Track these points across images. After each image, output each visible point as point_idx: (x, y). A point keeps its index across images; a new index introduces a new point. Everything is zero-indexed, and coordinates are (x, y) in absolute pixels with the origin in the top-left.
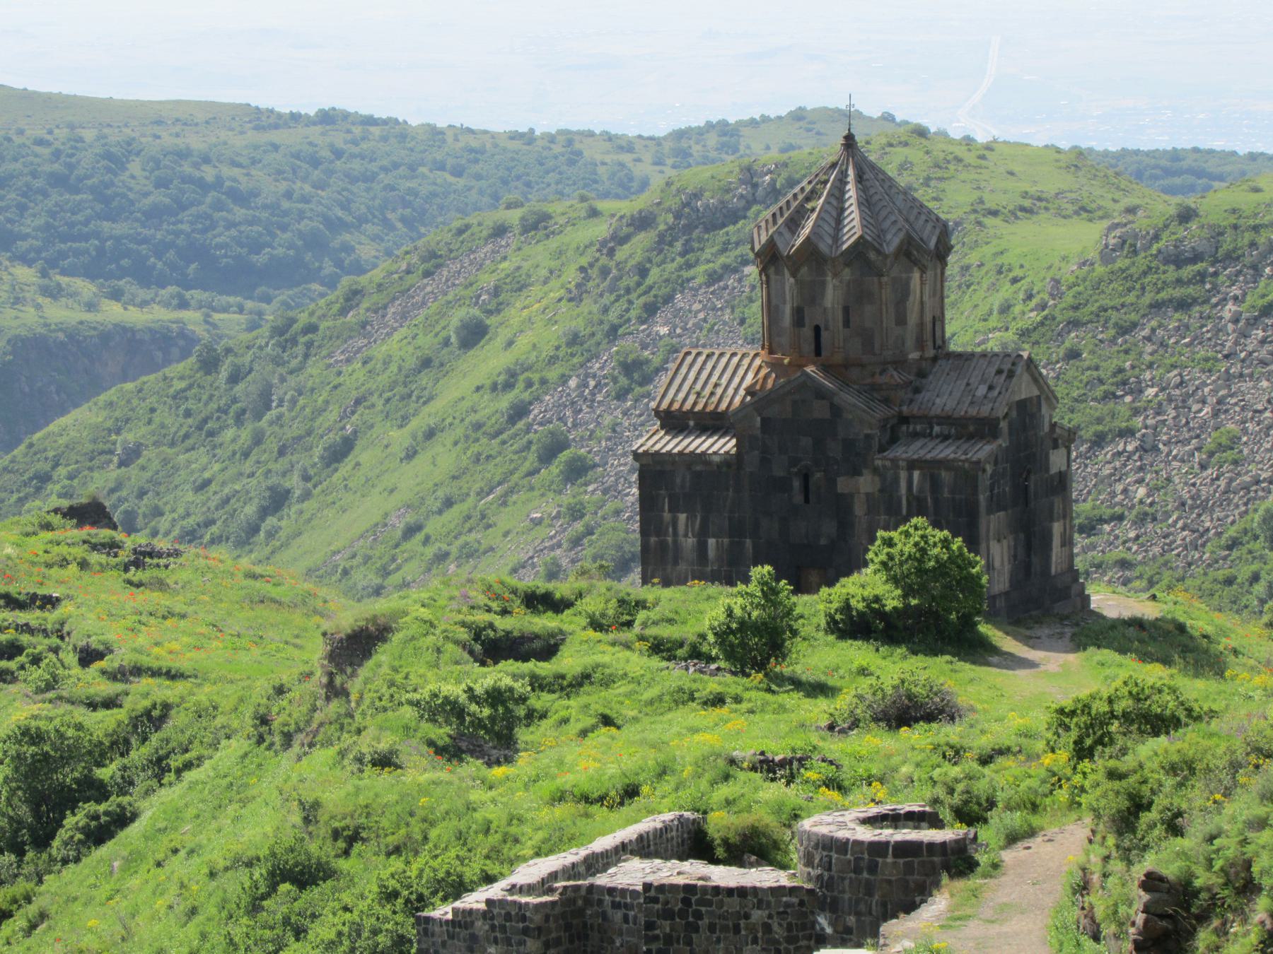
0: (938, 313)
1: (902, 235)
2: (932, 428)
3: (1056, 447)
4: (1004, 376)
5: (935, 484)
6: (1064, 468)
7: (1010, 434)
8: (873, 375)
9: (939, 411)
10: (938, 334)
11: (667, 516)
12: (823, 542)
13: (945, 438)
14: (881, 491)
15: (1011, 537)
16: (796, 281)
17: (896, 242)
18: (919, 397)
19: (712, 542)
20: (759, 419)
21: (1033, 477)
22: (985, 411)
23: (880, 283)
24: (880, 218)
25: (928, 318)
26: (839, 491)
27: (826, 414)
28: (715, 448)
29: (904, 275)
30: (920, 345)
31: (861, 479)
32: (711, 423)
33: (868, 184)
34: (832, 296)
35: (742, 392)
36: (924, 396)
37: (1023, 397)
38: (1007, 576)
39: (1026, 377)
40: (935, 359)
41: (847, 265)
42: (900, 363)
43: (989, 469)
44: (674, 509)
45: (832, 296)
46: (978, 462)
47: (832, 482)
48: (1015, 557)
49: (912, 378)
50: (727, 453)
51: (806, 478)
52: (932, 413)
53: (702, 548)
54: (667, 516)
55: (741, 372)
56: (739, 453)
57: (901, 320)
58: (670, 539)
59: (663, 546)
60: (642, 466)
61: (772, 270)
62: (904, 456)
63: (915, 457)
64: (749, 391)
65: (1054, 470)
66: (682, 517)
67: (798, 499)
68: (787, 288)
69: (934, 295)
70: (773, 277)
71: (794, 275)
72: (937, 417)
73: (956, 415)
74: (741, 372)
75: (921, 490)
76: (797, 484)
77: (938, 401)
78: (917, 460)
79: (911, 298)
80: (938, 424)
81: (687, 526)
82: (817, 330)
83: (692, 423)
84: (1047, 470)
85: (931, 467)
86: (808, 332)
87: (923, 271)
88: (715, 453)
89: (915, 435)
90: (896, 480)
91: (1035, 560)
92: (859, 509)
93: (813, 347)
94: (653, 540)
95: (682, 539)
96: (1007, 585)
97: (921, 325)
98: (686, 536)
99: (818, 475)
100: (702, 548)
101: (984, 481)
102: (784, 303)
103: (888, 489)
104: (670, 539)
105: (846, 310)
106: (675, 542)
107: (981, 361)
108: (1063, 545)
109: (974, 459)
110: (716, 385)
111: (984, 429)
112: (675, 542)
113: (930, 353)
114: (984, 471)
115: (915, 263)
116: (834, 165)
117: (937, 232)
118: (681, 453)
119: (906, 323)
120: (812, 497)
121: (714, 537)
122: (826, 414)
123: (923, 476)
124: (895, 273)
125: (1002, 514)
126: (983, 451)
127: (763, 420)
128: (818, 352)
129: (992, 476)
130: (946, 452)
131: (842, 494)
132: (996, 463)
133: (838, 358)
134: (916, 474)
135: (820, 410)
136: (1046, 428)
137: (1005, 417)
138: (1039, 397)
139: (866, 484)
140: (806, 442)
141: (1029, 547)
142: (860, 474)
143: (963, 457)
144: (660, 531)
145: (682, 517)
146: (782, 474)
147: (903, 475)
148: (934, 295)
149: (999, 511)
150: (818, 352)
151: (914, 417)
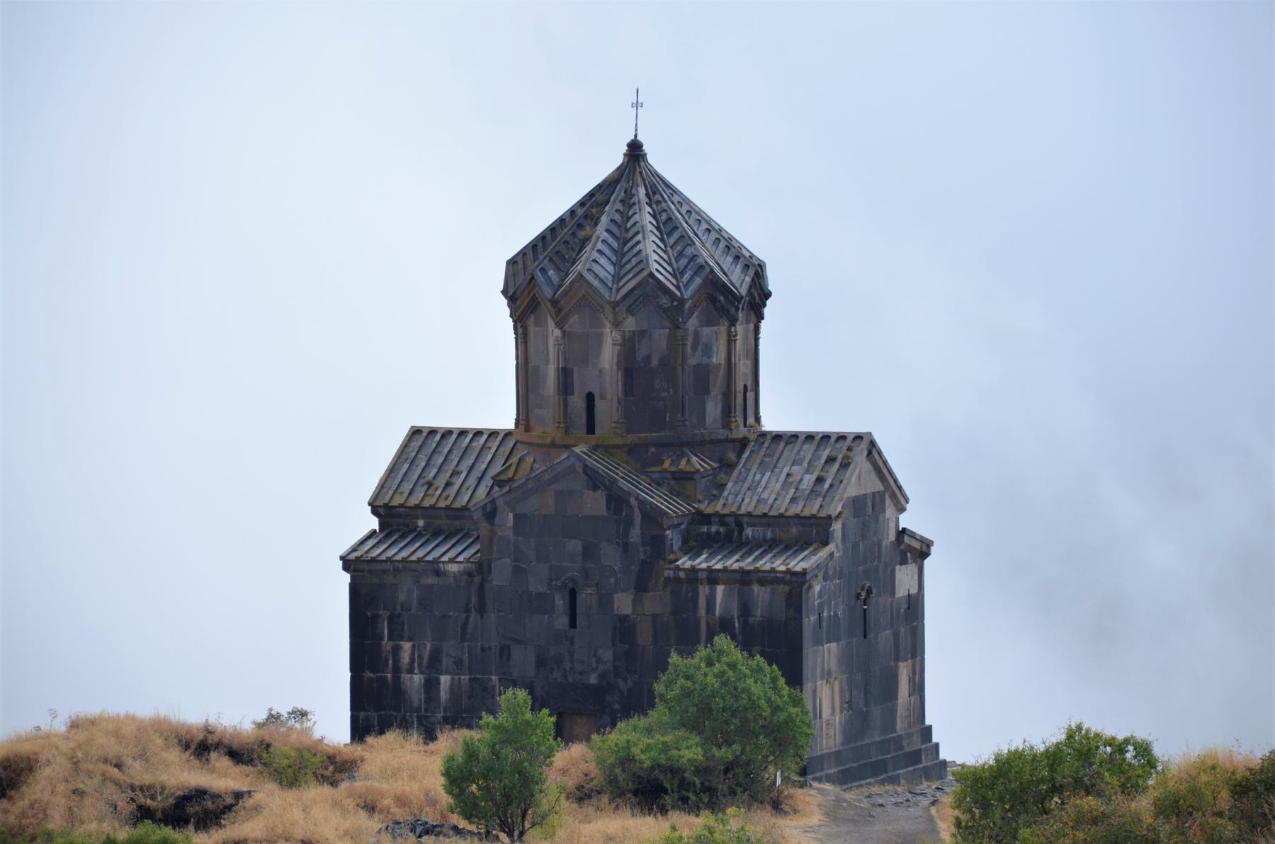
3: (904, 562)
4: (836, 466)
6: (914, 591)
16: (564, 333)
17: (698, 281)
19: (445, 680)
20: (511, 515)
22: (813, 508)
35: (488, 482)
39: (867, 466)
41: (630, 311)
46: (804, 573)
48: (850, 703)
53: (431, 686)
54: (387, 645)
64: (498, 482)
65: (901, 592)
66: (407, 646)
67: (562, 622)
68: (551, 343)
70: (532, 329)
71: (559, 325)
72: (749, 514)
76: (560, 602)
80: (750, 525)
81: (413, 654)
82: (590, 398)
83: (421, 523)
86: (578, 402)
91: (876, 711)
93: (583, 421)
95: (405, 677)
96: (839, 739)
98: (411, 671)
100: (431, 686)
102: (547, 363)
106: (397, 679)
111: (813, 531)
113: (741, 432)
117: (751, 272)
120: (580, 620)
121: (447, 673)
123: (727, 595)
125: (833, 645)
127: (515, 516)
128: (591, 429)
129: (820, 592)
134: (720, 589)
136: (892, 537)
137: (838, 517)
138: (881, 495)
140: (575, 545)
145: (407, 646)
146: (541, 589)
151: (716, 514)
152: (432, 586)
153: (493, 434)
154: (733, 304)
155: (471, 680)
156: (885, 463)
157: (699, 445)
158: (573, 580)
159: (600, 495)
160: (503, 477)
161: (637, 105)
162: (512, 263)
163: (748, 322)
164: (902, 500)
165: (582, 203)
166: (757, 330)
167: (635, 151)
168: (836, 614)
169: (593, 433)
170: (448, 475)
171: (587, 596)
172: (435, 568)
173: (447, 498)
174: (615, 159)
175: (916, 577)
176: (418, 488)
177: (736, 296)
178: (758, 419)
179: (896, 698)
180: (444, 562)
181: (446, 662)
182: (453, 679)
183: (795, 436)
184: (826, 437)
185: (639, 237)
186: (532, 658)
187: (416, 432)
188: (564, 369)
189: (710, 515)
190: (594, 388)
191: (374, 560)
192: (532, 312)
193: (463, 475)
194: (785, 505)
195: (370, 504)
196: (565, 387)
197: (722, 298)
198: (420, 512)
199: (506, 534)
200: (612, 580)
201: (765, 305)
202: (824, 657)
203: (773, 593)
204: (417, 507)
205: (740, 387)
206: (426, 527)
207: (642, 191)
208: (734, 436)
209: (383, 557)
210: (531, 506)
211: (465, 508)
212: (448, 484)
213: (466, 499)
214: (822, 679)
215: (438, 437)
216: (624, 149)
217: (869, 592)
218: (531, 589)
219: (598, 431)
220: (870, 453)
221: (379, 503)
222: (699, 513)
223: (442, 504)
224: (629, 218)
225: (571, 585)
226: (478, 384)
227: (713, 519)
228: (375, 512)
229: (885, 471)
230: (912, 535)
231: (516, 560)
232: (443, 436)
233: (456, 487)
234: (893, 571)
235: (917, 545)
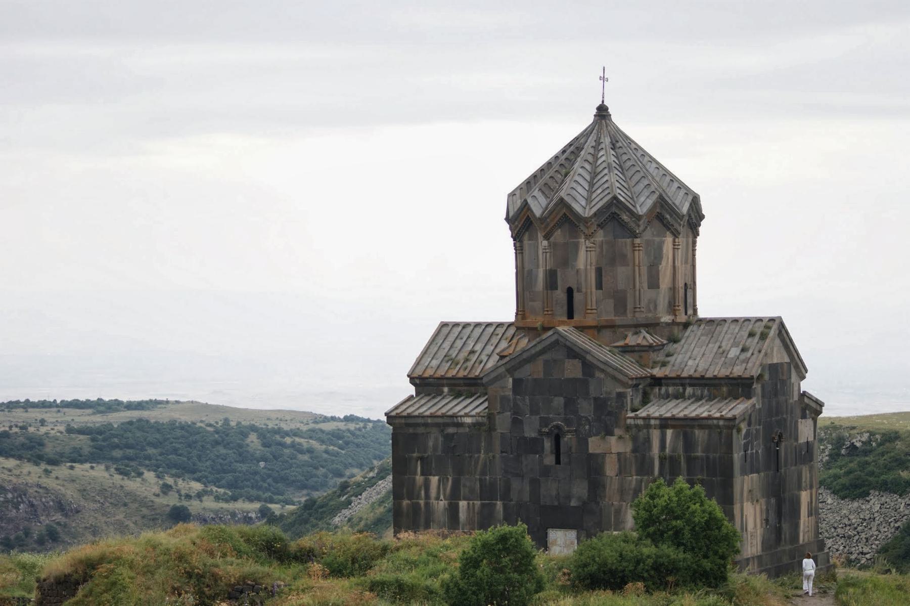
0: (689, 283)
1: (655, 197)
2: (685, 390)
3: (804, 417)
5: (689, 445)
6: (811, 439)
7: (763, 397)
8: (625, 337)
9: (691, 372)
10: (690, 300)
12: (573, 503)
13: (699, 399)
14: (634, 450)
15: (763, 501)
17: (649, 203)
18: (671, 359)
19: (463, 504)
20: (511, 380)
21: (783, 444)
23: (633, 245)
24: (633, 183)
25: (680, 284)
26: (590, 451)
27: (579, 375)
28: (467, 410)
29: (657, 239)
30: (672, 308)
31: (613, 440)
32: (466, 386)
33: (620, 151)
34: (585, 258)
36: (677, 359)
37: (775, 361)
38: (759, 540)
39: (778, 342)
40: (686, 325)
41: (601, 226)
42: (652, 326)
43: (744, 427)
44: (426, 473)
45: (585, 258)
46: (734, 419)
47: (583, 442)
48: (767, 520)
49: (665, 342)
50: (478, 414)
51: (557, 440)
52: (685, 375)
53: (453, 510)
54: (419, 479)
55: (495, 340)
56: (490, 417)
57: (654, 284)
58: (422, 502)
59: (415, 508)
60: (394, 429)
61: (526, 237)
62: (657, 414)
63: (669, 415)
65: (802, 440)
66: (434, 480)
67: (550, 460)
68: (540, 252)
69: (686, 262)
70: (526, 242)
71: (547, 237)
72: (690, 377)
73: (709, 375)
74: (495, 340)
75: (674, 450)
76: (548, 444)
77: (690, 363)
78: (673, 418)
79: (664, 263)
80: (691, 385)
82: (570, 291)
83: (446, 389)
84: (797, 439)
85: (685, 426)
86: (560, 295)
87: (676, 234)
88: (467, 415)
89: (667, 397)
90: (648, 440)
91: (785, 526)
92: (611, 469)
93: (565, 308)
94: (405, 502)
95: (433, 501)
96: (759, 548)
97: (673, 289)
98: (438, 498)
100: (453, 510)
101: (739, 441)
102: (538, 267)
103: (641, 448)
104: (422, 502)
105: (599, 271)
106: (427, 504)
107: (733, 326)
108: (810, 514)
109: (729, 415)
110: (472, 352)
111: (739, 387)
112: (427, 504)
113: (682, 318)
114: (739, 430)
115: (667, 227)
116: (586, 134)
117: (690, 198)
118: (432, 416)
119: (658, 287)
121: (465, 499)
122: (579, 375)
123: (676, 437)
124: (648, 235)
126: (738, 408)
127: (514, 381)
128: (570, 315)
130: (701, 410)
131: (591, 454)
132: (749, 424)
133: (590, 321)
134: (669, 433)
135: (573, 370)
136: (796, 398)
138: (789, 364)
139: (615, 446)
140: (559, 401)
141: (779, 514)
142: (612, 434)
143: (718, 415)
144: (412, 494)
145: (434, 480)
146: (533, 435)
147: (655, 435)
148: (686, 262)
149: (752, 473)
150: (570, 315)
151: (666, 378)
152: (453, 434)
153: (500, 325)
154: (676, 221)
155: (483, 505)
156: (791, 340)
157: (652, 326)
158: (558, 427)
159: (577, 363)
160: (505, 353)
161: (603, 79)
162: (512, 195)
163: (687, 236)
164: (803, 370)
165: (564, 151)
166: (694, 243)
167: (602, 112)
168: (757, 452)
169: (572, 318)
170: (466, 354)
171: (568, 439)
172: (453, 421)
173: (466, 369)
174: (587, 119)
175: (812, 429)
176: (444, 364)
177: (679, 217)
178: (695, 311)
179: (799, 518)
180: (461, 416)
181: (463, 491)
183: (724, 320)
184: (748, 320)
185: (606, 171)
186: (527, 488)
187: (444, 325)
188: (551, 270)
189: (660, 379)
190: (573, 284)
191: (409, 416)
192: (527, 230)
193: (477, 354)
194: (718, 369)
195: (408, 376)
197: (668, 216)
198: (445, 382)
199: (507, 393)
200: (587, 427)
201: (700, 225)
202: (746, 483)
203: (710, 435)
204: (442, 378)
206: (450, 391)
207: (607, 141)
208: (678, 320)
209: (416, 413)
210: (526, 372)
211: (476, 378)
212: (467, 360)
213: (479, 371)
214: (748, 500)
215: (460, 328)
216: (595, 111)
217: (780, 437)
218: (527, 435)
219: (577, 317)
220: (780, 332)
221: (415, 375)
222: (653, 377)
223: (461, 375)
224: (597, 159)
225: (556, 431)
226: (486, 286)
227: (663, 381)
229: (791, 347)
230: (810, 398)
231: (515, 413)
232: (464, 327)
233: (472, 362)
234: (796, 422)
235: (813, 405)
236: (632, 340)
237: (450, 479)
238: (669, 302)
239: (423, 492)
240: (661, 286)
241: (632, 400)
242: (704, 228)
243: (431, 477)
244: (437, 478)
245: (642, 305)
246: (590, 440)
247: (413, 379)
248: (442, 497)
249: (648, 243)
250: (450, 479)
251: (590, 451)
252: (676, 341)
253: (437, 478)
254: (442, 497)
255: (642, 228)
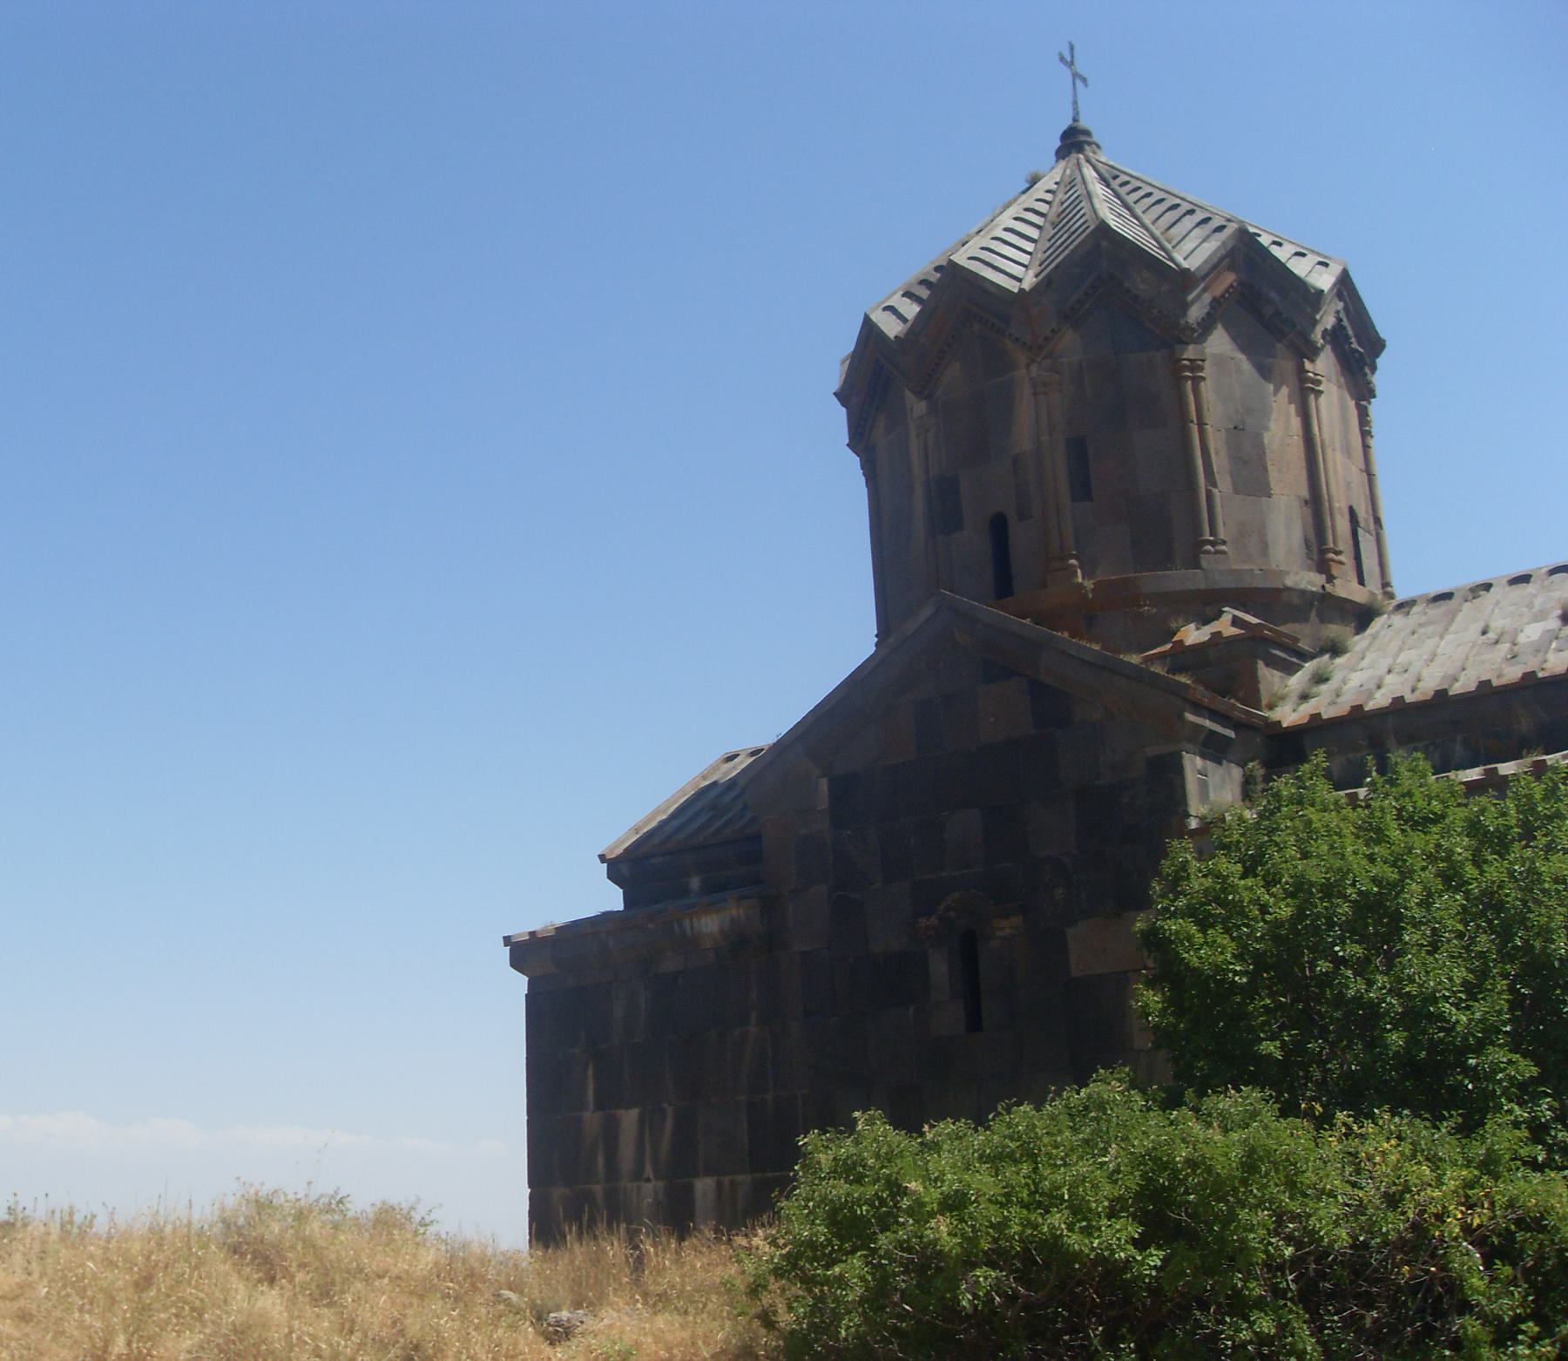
11: (591, 1119)
20: (824, 785)
26: (1075, 972)
30: (1320, 556)
34: (1034, 419)
44: (608, 1101)
45: (1034, 419)
51: (968, 949)
57: (1253, 482)
58: (598, 1189)
60: (531, 984)
66: (629, 1118)
69: (1347, 452)
76: (940, 967)
86: (973, 540)
97: (1315, 502)
98: (638, 1175)
99: (1007, 927)
105: (1078, 450)
121: (708, 1173)
150: (1003, 586)
169: (1011, 593)
182: (719, 1185)
189: (1297, 732)
196: (946, 516)
200: (1059, 892)
201: (1374, 369)
205: (1340, 504)
228: (612, 876)
236: (1193, 635)
237: (670, 1110)
238: (1306, 541)
239: (601, 1161)
240: (1276, 488)
241: (1203, 787)
242: (1385, 375)
243: (621, 1112)
244: (634, 1113)
245: (1222, 535)
246: (1070, 931)
247: (621, 867)
248: (649, 1171)
249: (1220, 361)
250: (670, 1110)
251: (1075, 972)
252: (1336, 650)
253: (634, 1113)
254: (649, 1171)
255: (1195, 313)
